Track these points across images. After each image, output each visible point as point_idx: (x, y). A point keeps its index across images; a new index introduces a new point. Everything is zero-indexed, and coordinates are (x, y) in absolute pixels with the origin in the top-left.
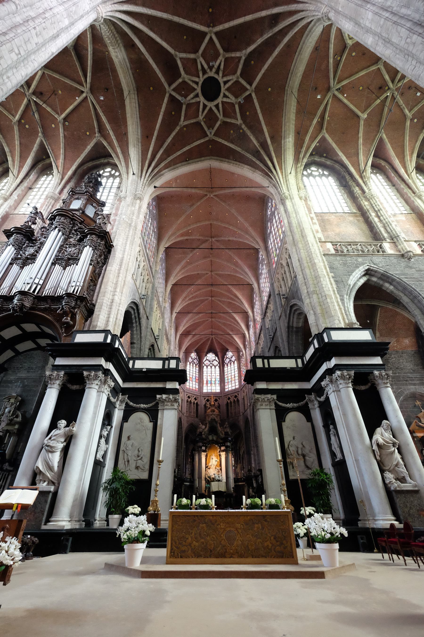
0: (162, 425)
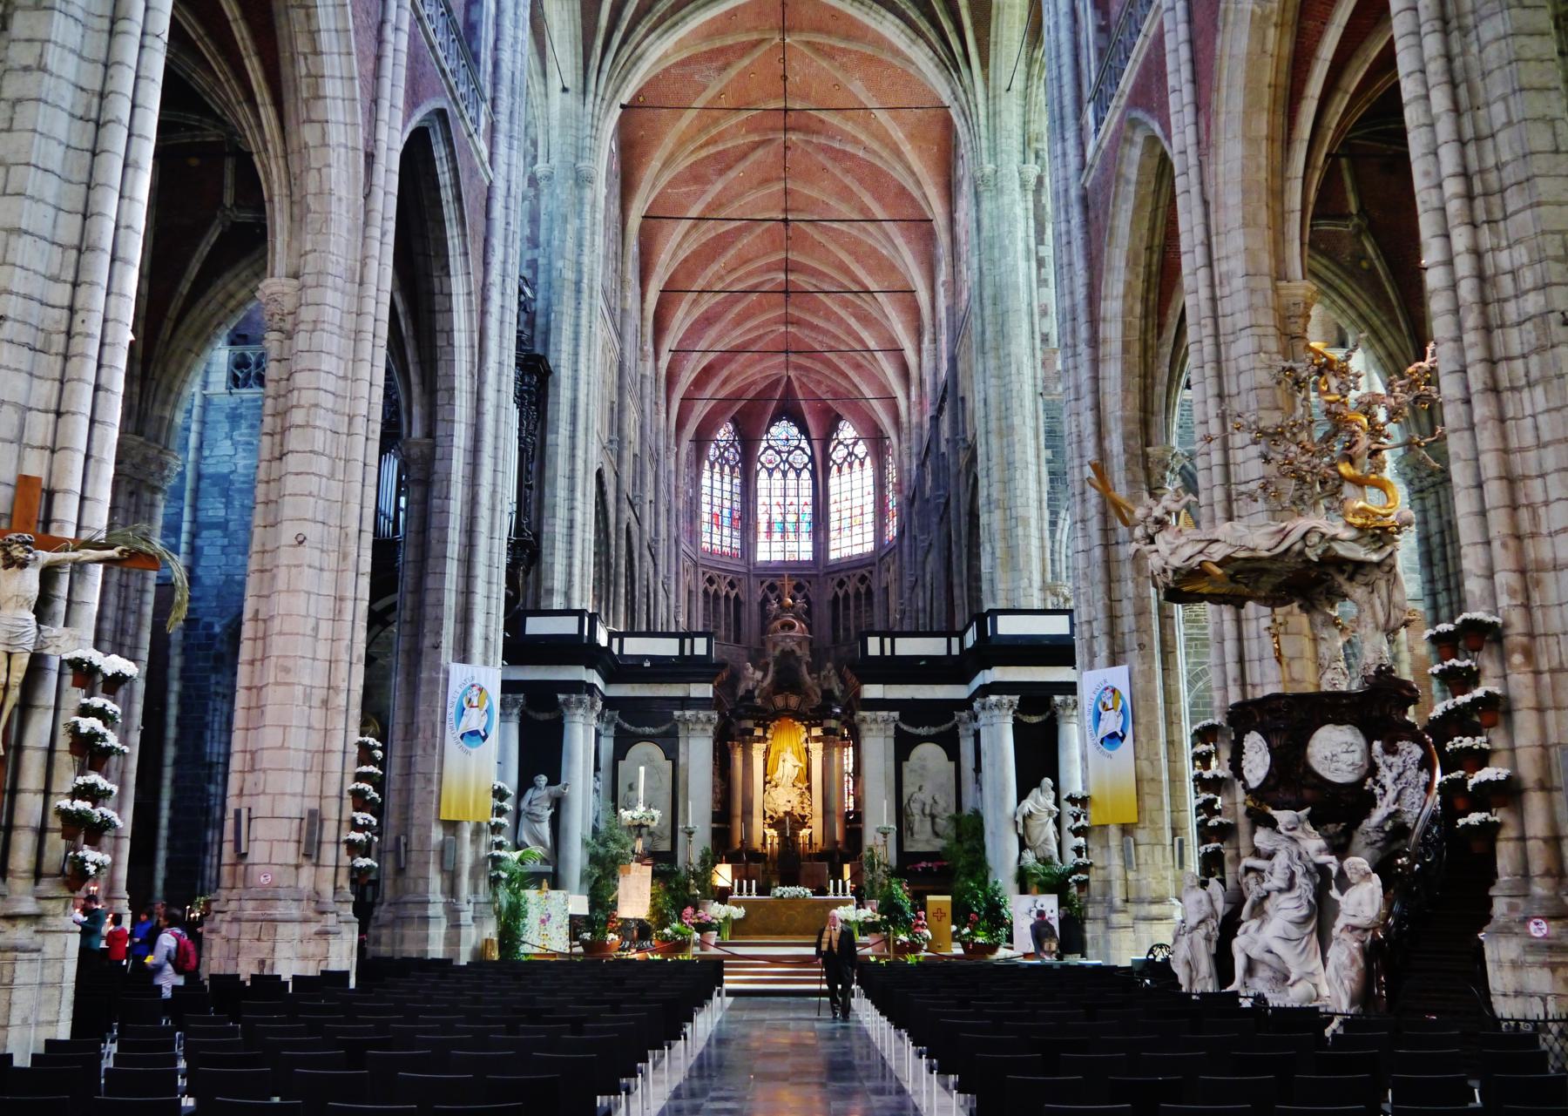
0: (687, 764)
